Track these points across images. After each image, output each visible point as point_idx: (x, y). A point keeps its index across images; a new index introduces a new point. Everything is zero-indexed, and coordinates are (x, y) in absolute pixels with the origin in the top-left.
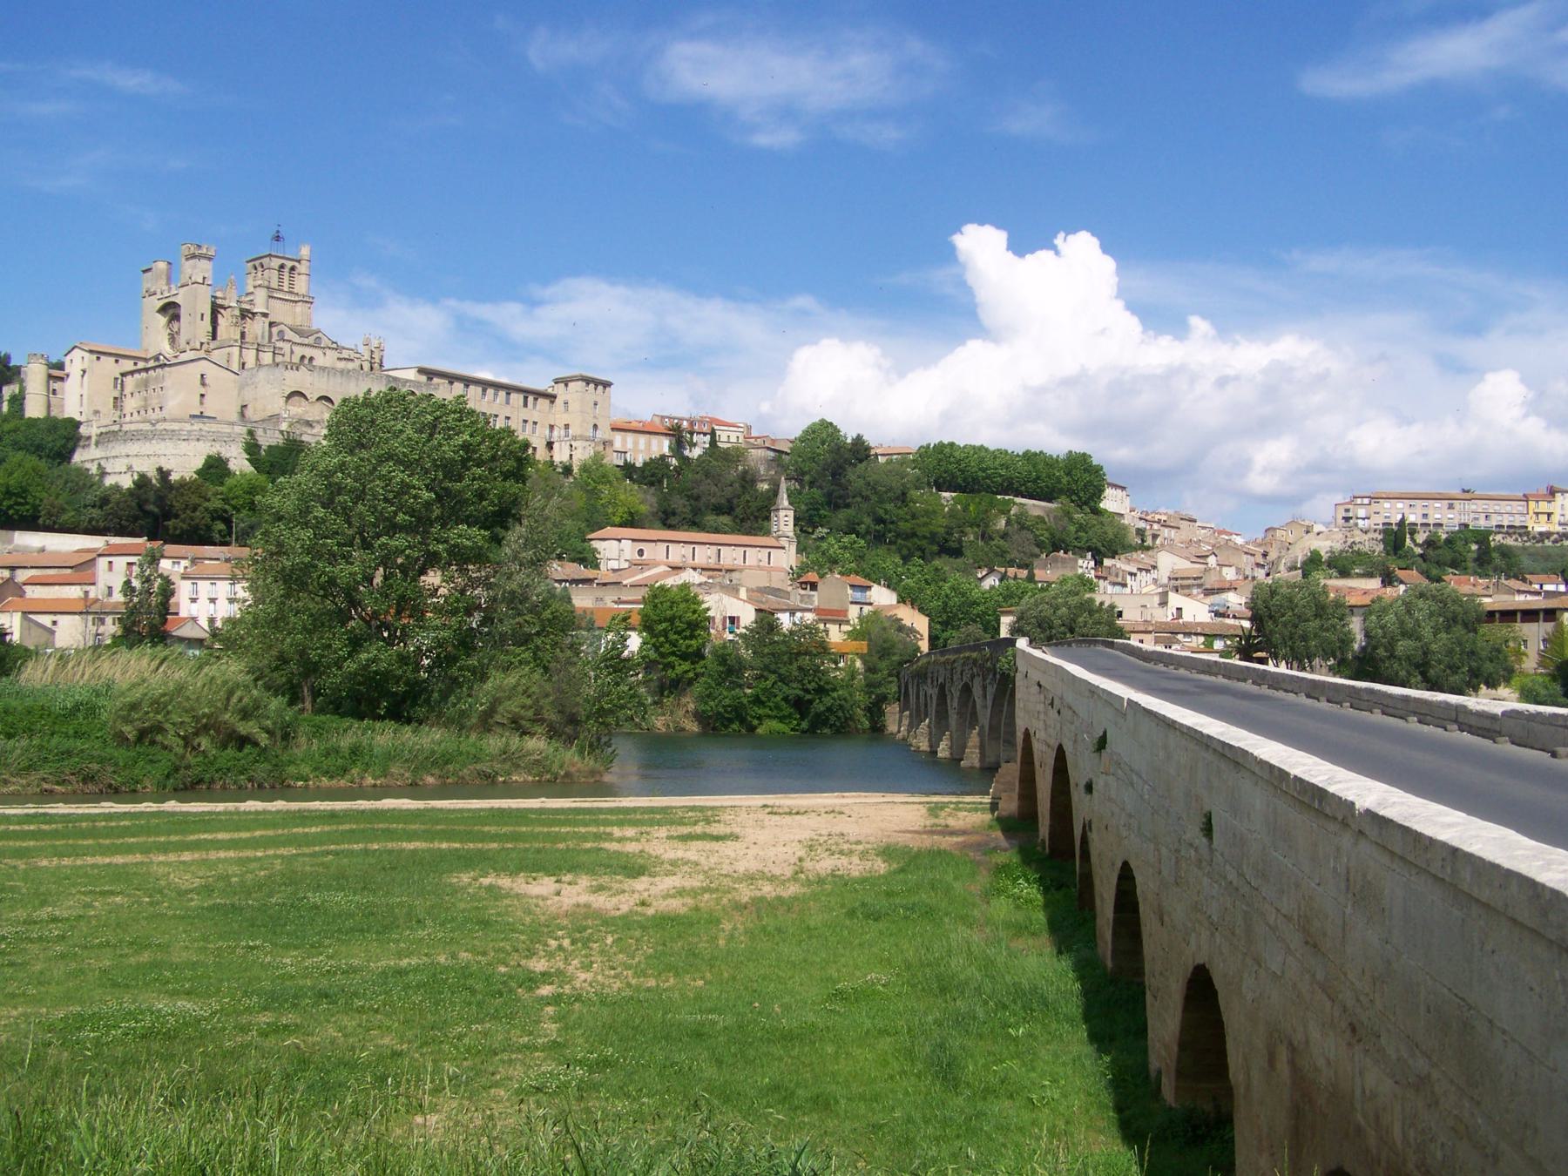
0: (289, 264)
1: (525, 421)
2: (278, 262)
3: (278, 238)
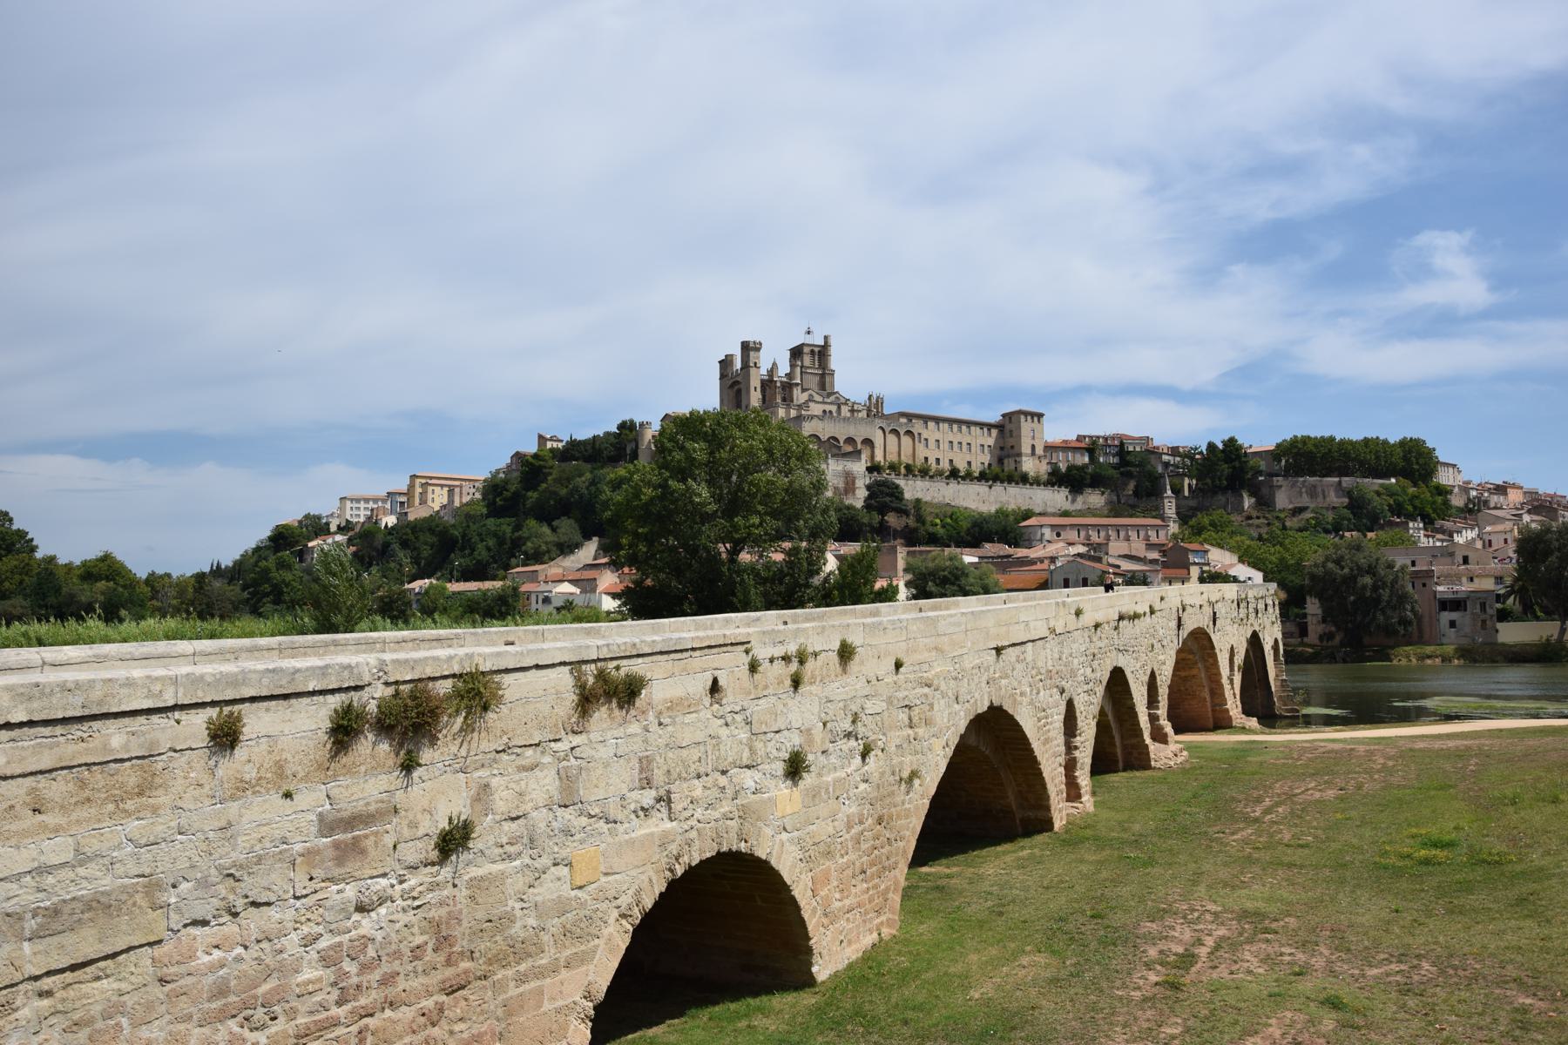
0: (817, 349)
1: (983, 446)
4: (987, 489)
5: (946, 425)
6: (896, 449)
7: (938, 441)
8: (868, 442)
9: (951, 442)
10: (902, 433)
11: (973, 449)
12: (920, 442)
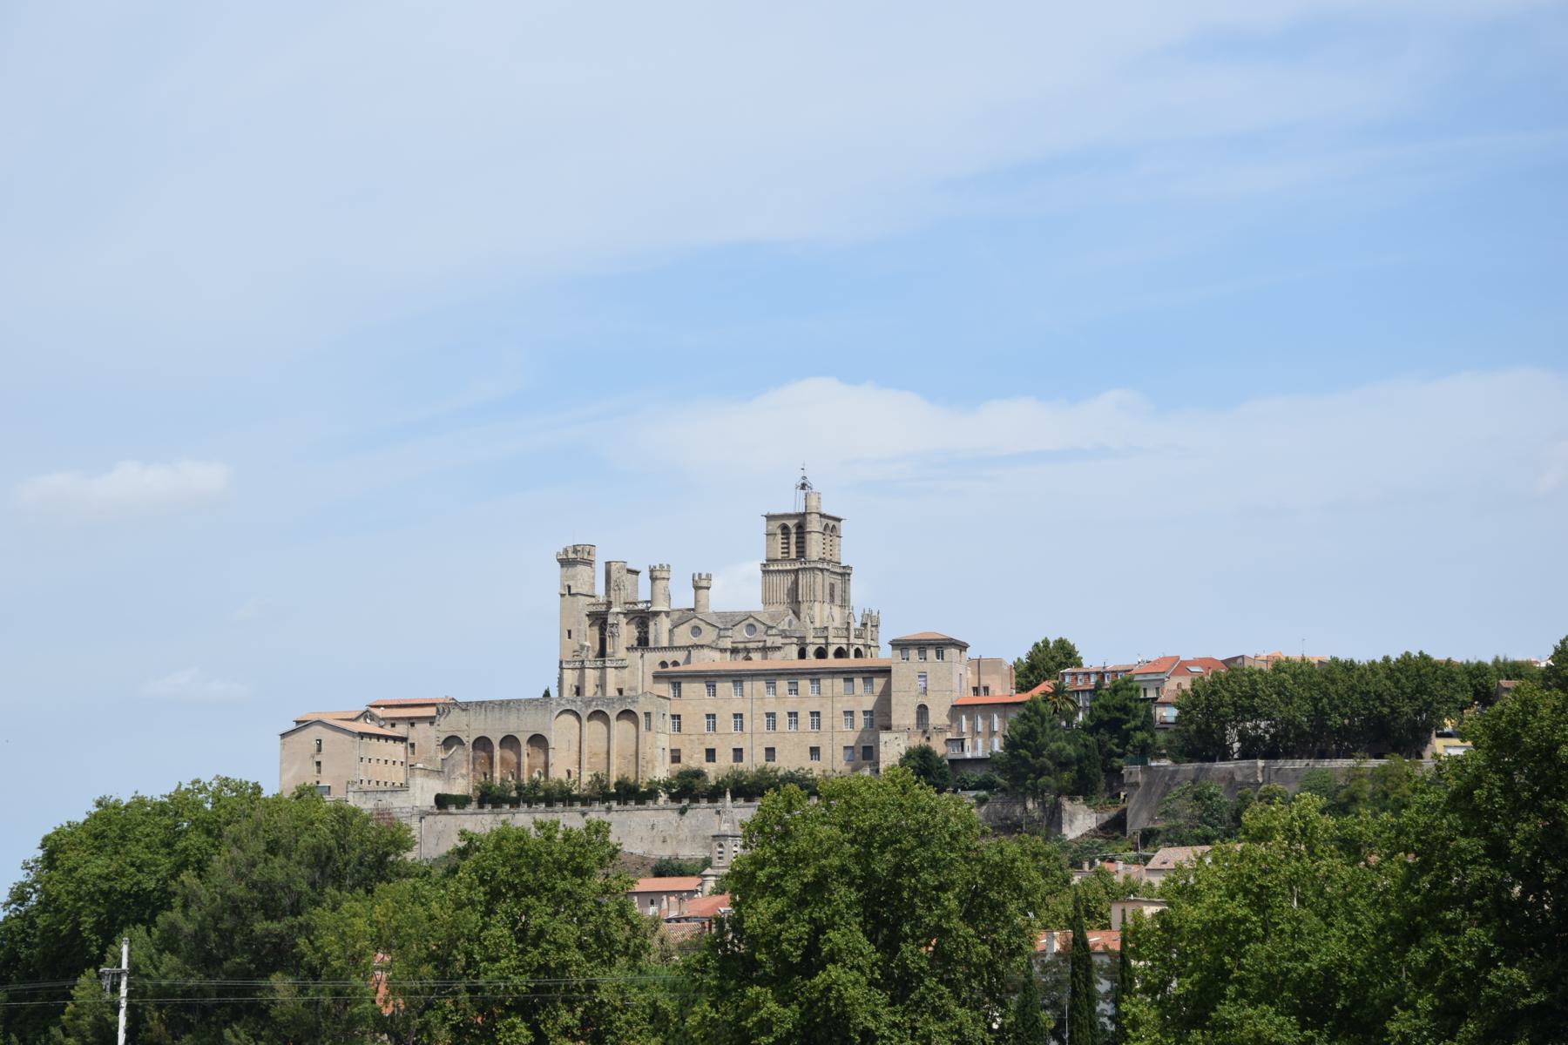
0: (791, 523)
3: (803, 486)
4: (674, 816)
5: (760, 685)
6: (606, 744)
7: (738, 716)
8: (539, 741)
9: (771, 715)
10: (613, 717)
11: (825, 722)
12: (649, 728)
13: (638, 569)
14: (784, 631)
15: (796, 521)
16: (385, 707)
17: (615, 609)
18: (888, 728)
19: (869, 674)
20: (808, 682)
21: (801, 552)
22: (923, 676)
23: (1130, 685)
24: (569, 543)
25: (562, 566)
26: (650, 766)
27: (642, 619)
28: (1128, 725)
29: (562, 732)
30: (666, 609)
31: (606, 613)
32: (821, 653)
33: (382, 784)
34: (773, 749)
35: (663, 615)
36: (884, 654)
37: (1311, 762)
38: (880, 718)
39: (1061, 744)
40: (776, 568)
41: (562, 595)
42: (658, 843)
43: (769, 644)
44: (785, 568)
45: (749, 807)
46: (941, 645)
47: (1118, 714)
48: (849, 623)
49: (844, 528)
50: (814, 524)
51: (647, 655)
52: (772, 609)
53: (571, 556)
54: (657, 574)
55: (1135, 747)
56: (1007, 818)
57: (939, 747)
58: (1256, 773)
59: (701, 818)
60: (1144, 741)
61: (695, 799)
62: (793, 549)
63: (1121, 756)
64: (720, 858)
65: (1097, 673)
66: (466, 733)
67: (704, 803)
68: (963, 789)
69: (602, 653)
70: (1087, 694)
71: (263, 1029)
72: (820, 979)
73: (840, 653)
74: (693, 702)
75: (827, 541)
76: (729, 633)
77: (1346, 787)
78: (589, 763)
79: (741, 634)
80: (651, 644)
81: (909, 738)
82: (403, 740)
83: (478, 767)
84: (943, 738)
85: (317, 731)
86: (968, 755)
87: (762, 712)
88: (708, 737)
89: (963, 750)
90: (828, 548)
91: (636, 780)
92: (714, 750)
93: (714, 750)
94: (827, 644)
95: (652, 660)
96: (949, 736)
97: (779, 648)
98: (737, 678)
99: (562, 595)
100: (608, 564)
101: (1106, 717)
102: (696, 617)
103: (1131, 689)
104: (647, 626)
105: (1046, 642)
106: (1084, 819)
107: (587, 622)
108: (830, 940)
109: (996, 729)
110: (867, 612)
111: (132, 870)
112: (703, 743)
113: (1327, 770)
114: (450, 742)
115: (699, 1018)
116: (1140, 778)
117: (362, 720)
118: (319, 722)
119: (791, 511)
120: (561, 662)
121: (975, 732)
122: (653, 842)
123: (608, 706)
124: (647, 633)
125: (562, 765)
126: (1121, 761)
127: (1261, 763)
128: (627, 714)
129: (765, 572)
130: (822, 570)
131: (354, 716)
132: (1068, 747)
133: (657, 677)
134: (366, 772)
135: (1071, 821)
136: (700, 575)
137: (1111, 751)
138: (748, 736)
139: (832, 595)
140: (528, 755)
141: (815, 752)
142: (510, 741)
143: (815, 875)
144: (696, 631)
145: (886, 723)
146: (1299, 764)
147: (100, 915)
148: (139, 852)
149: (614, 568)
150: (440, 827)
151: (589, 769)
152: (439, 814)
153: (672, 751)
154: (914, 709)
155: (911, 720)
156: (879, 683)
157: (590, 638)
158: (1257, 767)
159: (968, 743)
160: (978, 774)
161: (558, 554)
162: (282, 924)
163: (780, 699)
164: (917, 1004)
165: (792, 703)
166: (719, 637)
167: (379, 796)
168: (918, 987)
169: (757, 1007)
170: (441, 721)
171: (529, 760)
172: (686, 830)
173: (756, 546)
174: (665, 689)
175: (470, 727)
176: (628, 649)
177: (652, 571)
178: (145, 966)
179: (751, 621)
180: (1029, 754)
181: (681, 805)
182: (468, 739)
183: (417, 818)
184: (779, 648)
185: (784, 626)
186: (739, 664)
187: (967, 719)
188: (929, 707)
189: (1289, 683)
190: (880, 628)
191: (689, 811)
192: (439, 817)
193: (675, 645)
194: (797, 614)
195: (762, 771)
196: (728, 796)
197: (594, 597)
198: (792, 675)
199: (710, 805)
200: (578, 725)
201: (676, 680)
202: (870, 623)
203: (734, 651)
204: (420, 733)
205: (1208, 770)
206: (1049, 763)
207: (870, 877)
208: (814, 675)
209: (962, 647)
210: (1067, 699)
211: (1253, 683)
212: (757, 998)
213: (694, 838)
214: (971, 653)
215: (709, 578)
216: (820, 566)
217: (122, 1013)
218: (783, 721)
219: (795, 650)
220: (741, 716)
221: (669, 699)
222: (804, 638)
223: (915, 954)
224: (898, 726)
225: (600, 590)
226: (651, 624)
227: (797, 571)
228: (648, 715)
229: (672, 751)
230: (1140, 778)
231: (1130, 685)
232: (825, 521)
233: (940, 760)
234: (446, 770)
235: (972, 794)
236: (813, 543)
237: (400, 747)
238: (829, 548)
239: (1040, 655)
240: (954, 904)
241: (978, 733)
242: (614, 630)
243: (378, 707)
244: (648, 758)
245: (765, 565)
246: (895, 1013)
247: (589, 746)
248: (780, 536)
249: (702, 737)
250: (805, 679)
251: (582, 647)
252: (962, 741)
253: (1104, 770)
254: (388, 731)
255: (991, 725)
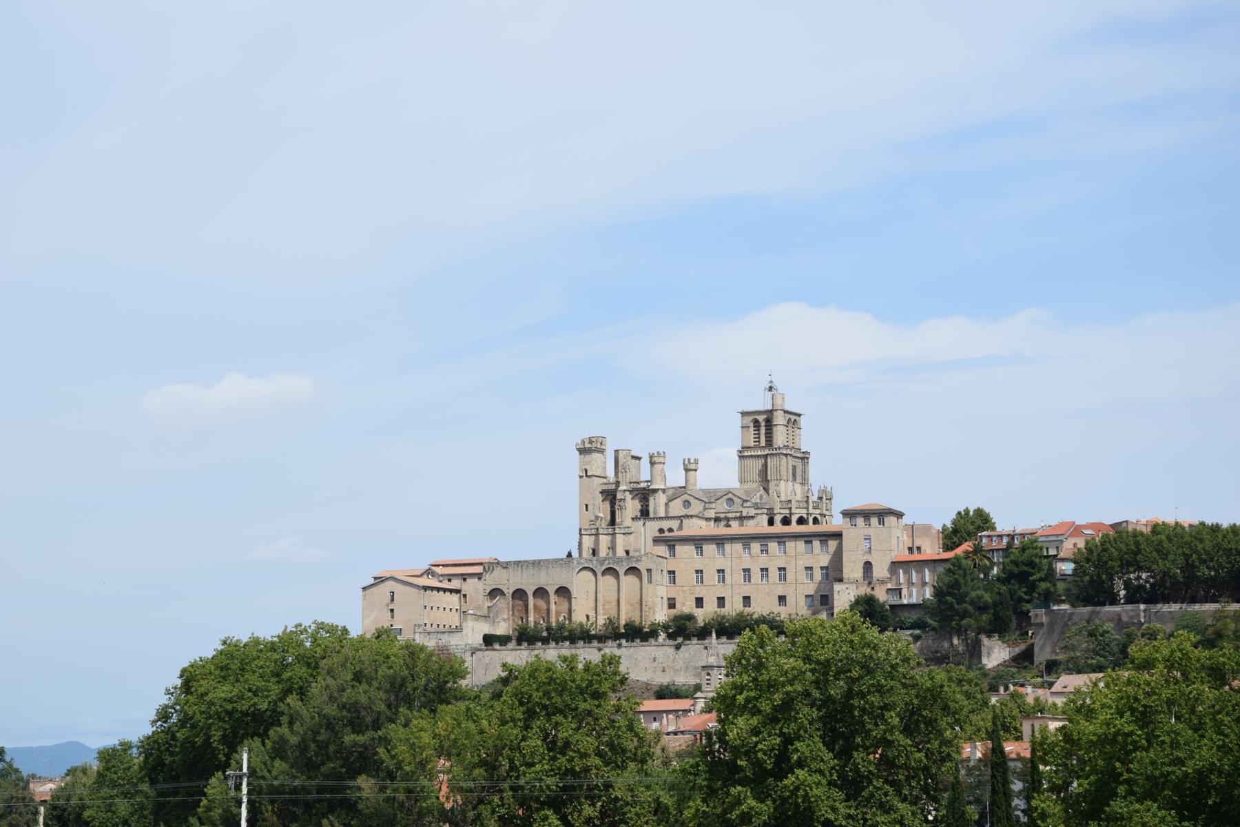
0: (761, 418)
2: (751, 418)
3: (771, 389)
4: (671, 651)
5: (738, 547)
8: (563, 592)
9: (747, 571)
10: (621, 572)
11: (790, 576)
12: (650, 581)
13: (640, 456)
14: (756, 503)
15: (765, 417)
16: (443, 566)
17: (622, 488)
18: (840, 580)
19: (825, 537)
20: (776, 544)
21: (769, 442)
22: (868, 539)
23: (1035, 545)
24: (586, 436)
25: (580, 454)
26: (652, 612)
27: (644, 495)
28: (1034, 577)
29: (581, 585)
30: (662, 487)
31: (615, 490)
32: (786, 521)
33: (441, 626)
34: (749, 598)
35: (660, 492)
36: (836, 522)
37: (1184, 606)
38: (834, 572)
39: (979, 592)
40: (749, 454)
41: (581, 477)
42: (659, 673)
43: (744, 514)
44: (756, 453)
45: (731, 643)
46: (882, 514)
47: (1025, 568)
48: (808, 497)
49: (803, 421)
50: (779, 419)
51: (648, 523)
52: (747, 486)
53: (587, 445)
54: (655, 459)
55: (1039, 594)
56: (937, 652)
57: (881, 595)
58: (1139, 615)
59: (692, 653)
60: (1047, 589)
61: (687, 637)
62: (763, 438)
63: (1028, 602)
64: (708, 684)
65: (1008, 535)
66: (507, 586)
67: (695, 641)
68: (902, 628)
69: (613, 522)
70: (1001, 552)
71: (352, 819)
72: (790, 780)
73: (801, 521)
74: (685, 560)
75: (790, 432)
76: (713, 505)
77: (1213, 626)
78: (604, 609)
79: (722, 506)
80: (651, 515)
81: (857, 588)
82: (458, 591)
83: (516, 612)
84: (884, 588)
85: (390, 586)
86: (905, 601)
87: (740, 568)
88: (697, 588)
89: (900, 598)
90: (791, 437)
91: (641, 623)
92: (702, 599)
93: (702, 599)
94: (791, 514)
95: (652, 527)
96: (889, 586)
97: (752, 517)
98: (720, 541)
99: (581, 477)
100: (616, 451)
101: (1016, 570)
102: (686, 493)
103: (1036, 548)
104: (648, 501)
105: (967, 511)
106: (1000, 652)
107: (600, 497)
108: (797, 750)
109: (927, 580)
110: (822, 488)
111: (250, 694)
112: (692, 593)
113: (1197, 613)
114: (495, 593)
115: (693, 811)
116: (1044, 619)
117: (425, 576)
118: (392, 578)
119: (761, 408)
120: (580, 530)
121: (910, 583)
122: (655, 671)
123: (618, 563)
124: (648, 506)
125: (582, 611)
126: (1028, 606)
127: (1142, 607)
128: (633, 570)
129: (740, 457)
130: (786, 455)
131: (419, 573)
132: (985, 595)
133: (656, 541)
134: (429, 617)
135: (989, 653)
136: (689, 459)
137: (1020, 597)
138: (730, 588)
139: (794, 475)
140: (555, 603)
141: (782, 599)
142: (541, 592)
143: (781, 700)
144: (687, 504)
145: (839, 576)
146: (1175, 607)
147: (226, 730)
148: (254, 680)
149: (621, 455)
150: (487, 660)
151: (603, 614)
152: (486, 650)
153: (669, 599)
154: (861, 565)
155: (858, 573)
156: (833, 544)
157: (603, 511)
158: (1139, 610)
159: (905, 592)
160: (913, 617)
161: (577, 444)
162: (366, 736)
163: (754, 557)
164: (868, 800)
165: (763, 561)
166: (705, 509)
167: (440, 636)
168: (867, 787)
169: (739, 802)
170: (487, 576)
171: (556, 607)
172: (681, 662)
173: (733, 437)
174: (662, 550)
175: (510, 582)
176: (633, 519)
177: (651, 457)
178: (261, 770)
179: (730, 496)
180: (954, 601)
181: (676, 642)
182: (509, 591)
183: (469, 654)
184: (752, 517)
185: (756, 499)
186: (721, 530)
187: (904, 573)
188: (873, 563)
189: (1166, 544)
190: (833, 501)
191: (682, 647)
192: (487, 652)
193: (670, 515)
194: (766, 490)
195: (741, 615)
196: (714, 635)
197: (606, 478)
198: (764, 538)
199: (700, 642)
200: (594, 579)
201: (669, 542)
202: (825, 497)
203: (717, 520)
204: (470, 586)
205: (1099, 613)
206: (970, 608)
207: (828, 700)
208: (781, 539)
209: (899, 515)
210: (985, 556)
211: (1137, 544)
212: (739, 795)
213: (687, 668)
214: (906, 520)
215: (696, 462)
216: (785, 452)
217: (244, 806)
218: (756, 575)
219: (765, 519)
220: (723, 571)
221: (666, 558)
222: (772, 509)
223: (866, 760)
224: (849, 579)
225: (610, 473)
226: (651, 499)
227: (766, 456)
228: (649, 571)
229: (669, 599)
230: (1044, 619)
231: (1035, 545)
232: (788, 416)
233: (882, 606)
234: (491, 615)
235: (909, 632)
236: (779, 433)
237: (455, 597)
238: (791, 437)
239: (962, 521)
240: (896, 721)
241: (913, 584)
242: (622, 504)
243: (438, 566)
244: (650, 604)
245: (741, 452)
246: (850, 807)
247: (603, 596)
248: (752, 429)
249: (693, 588)
250: (774, 541)
251: (597, 517)
252: (900, 591)
253: (1014, 613)
254: (445, 585)
255: (923, 577)
